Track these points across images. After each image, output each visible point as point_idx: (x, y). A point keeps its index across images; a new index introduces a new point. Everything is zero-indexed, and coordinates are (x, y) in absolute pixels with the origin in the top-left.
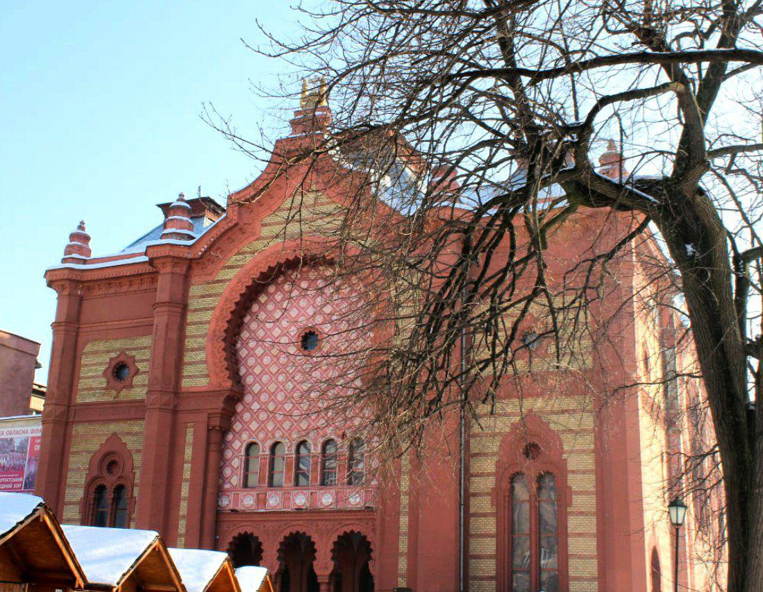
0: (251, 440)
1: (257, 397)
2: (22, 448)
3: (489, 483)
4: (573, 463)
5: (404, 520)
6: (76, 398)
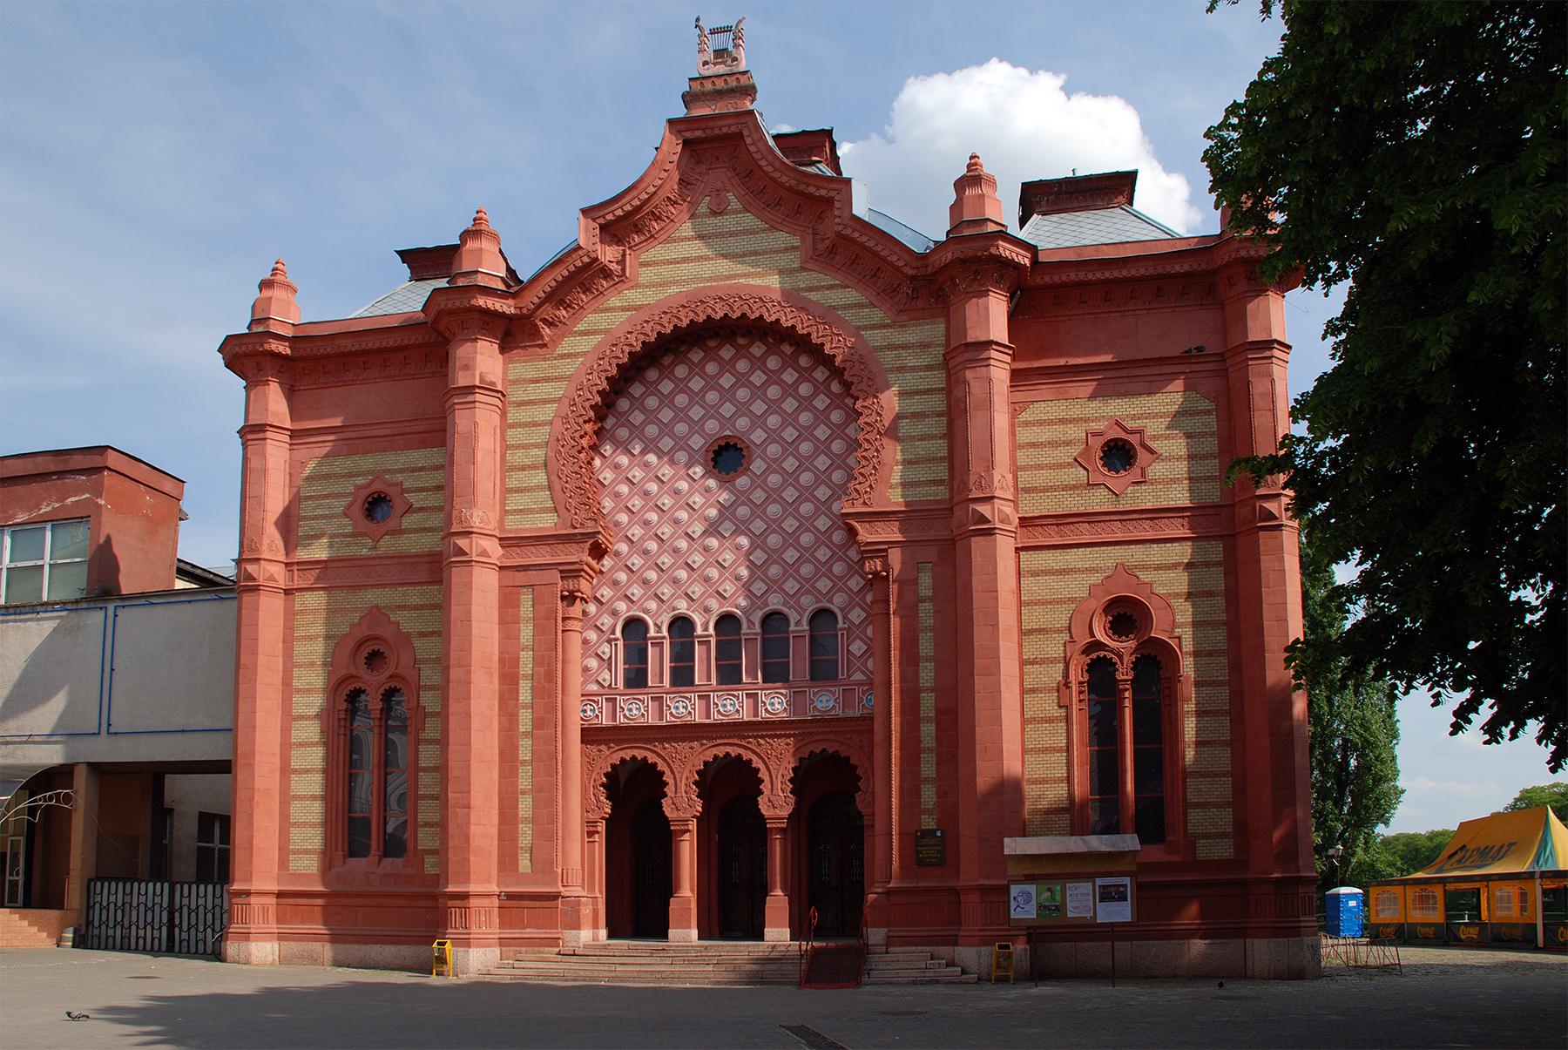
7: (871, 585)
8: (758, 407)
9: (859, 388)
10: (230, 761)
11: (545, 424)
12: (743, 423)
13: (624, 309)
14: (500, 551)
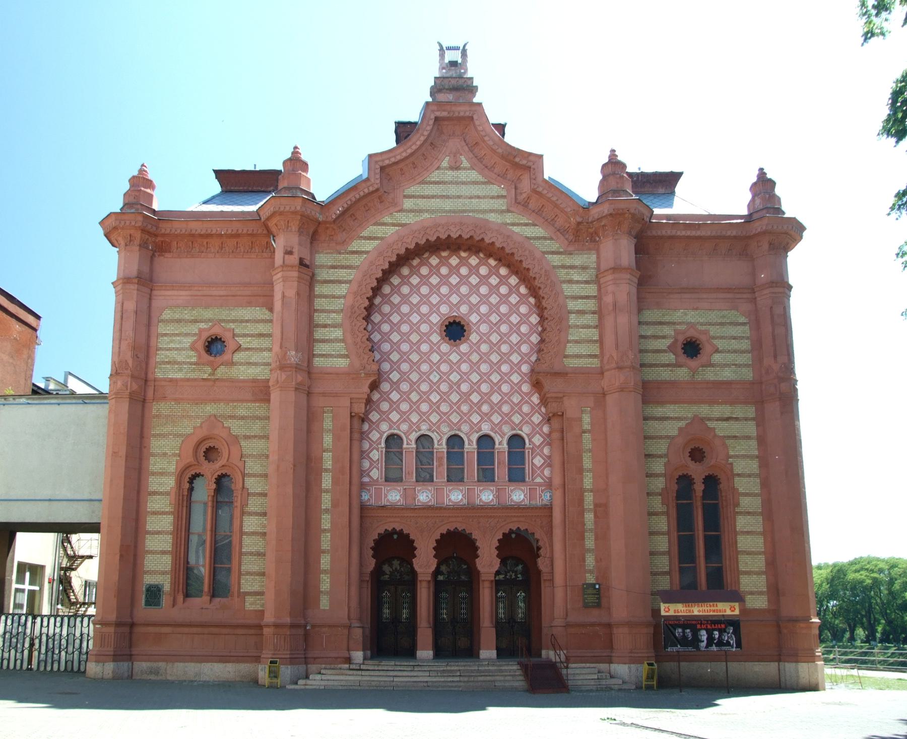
1: (395, 386)
3: (659, 484)
4: (739, 466)
5: (589, 517)
7: (549, 420)
8: (474, 299)
10: (100, 523)
12: (464, 309)
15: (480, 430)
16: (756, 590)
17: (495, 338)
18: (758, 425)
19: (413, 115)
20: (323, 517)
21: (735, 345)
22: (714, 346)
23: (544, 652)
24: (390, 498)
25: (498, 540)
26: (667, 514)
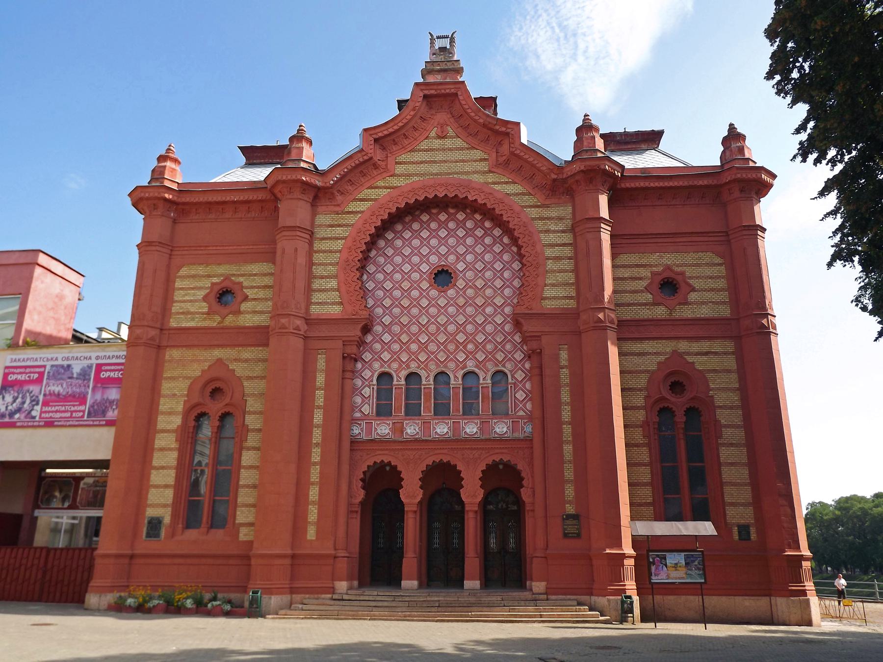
0: (383, 369)
2: (84, 375)
4: (720, 399)
5: (568, 449)
6: (169, 322)
7: (529, 357)
8: (461, 250)
9: (523, 241)
11: (337, 252)
12: (452, 258)
13: (386, 188)
14: (306, 327)
15: (465, 367)
16: (744, 522)
17: (479, 283)
18: (737, 359)
19: (407, 96)
20: (313, 450)
21: (711, 284)
22: (689, 285)
23: (528, 583)
24: (379, 431)
25: (482, 471)
26: (648, 445)
